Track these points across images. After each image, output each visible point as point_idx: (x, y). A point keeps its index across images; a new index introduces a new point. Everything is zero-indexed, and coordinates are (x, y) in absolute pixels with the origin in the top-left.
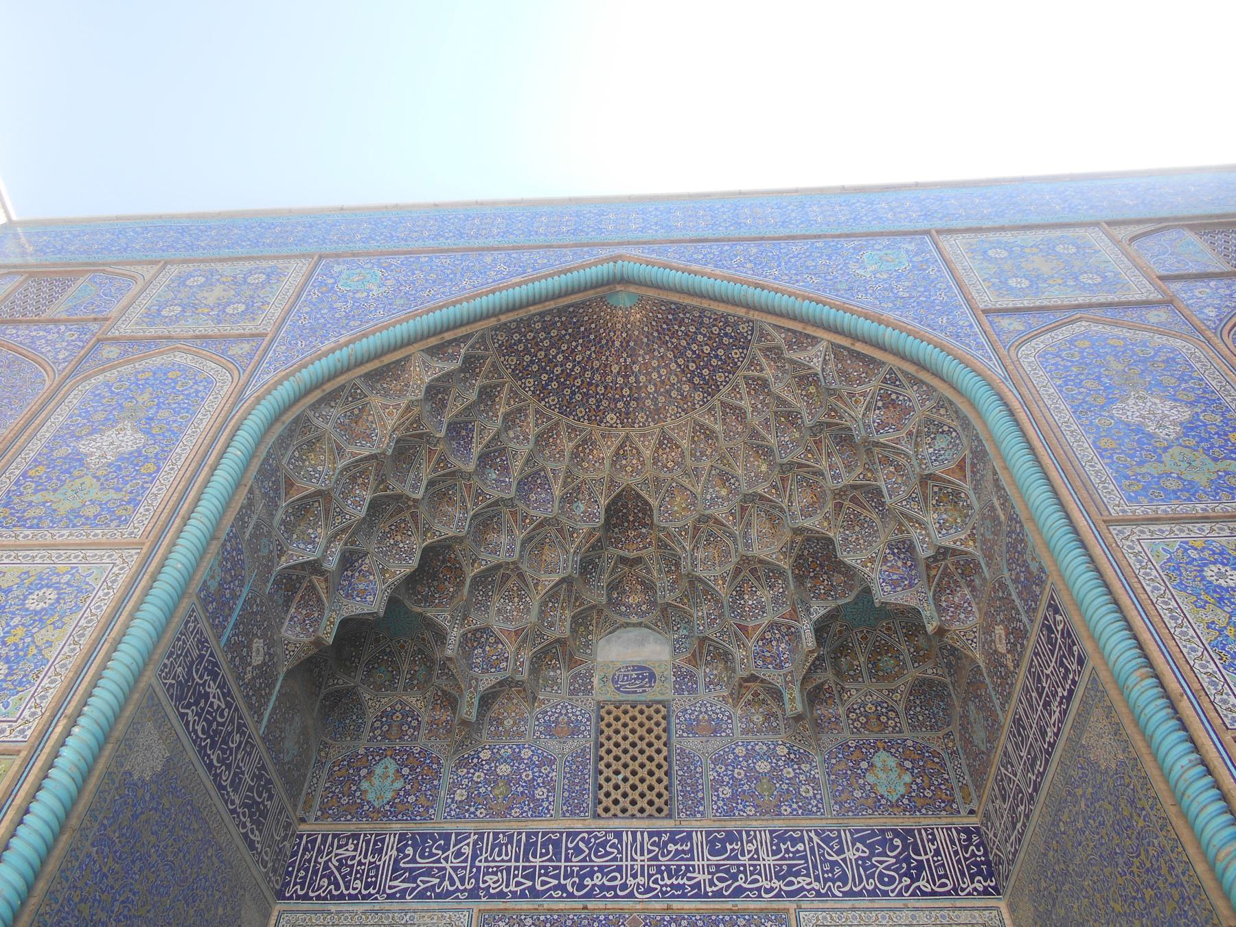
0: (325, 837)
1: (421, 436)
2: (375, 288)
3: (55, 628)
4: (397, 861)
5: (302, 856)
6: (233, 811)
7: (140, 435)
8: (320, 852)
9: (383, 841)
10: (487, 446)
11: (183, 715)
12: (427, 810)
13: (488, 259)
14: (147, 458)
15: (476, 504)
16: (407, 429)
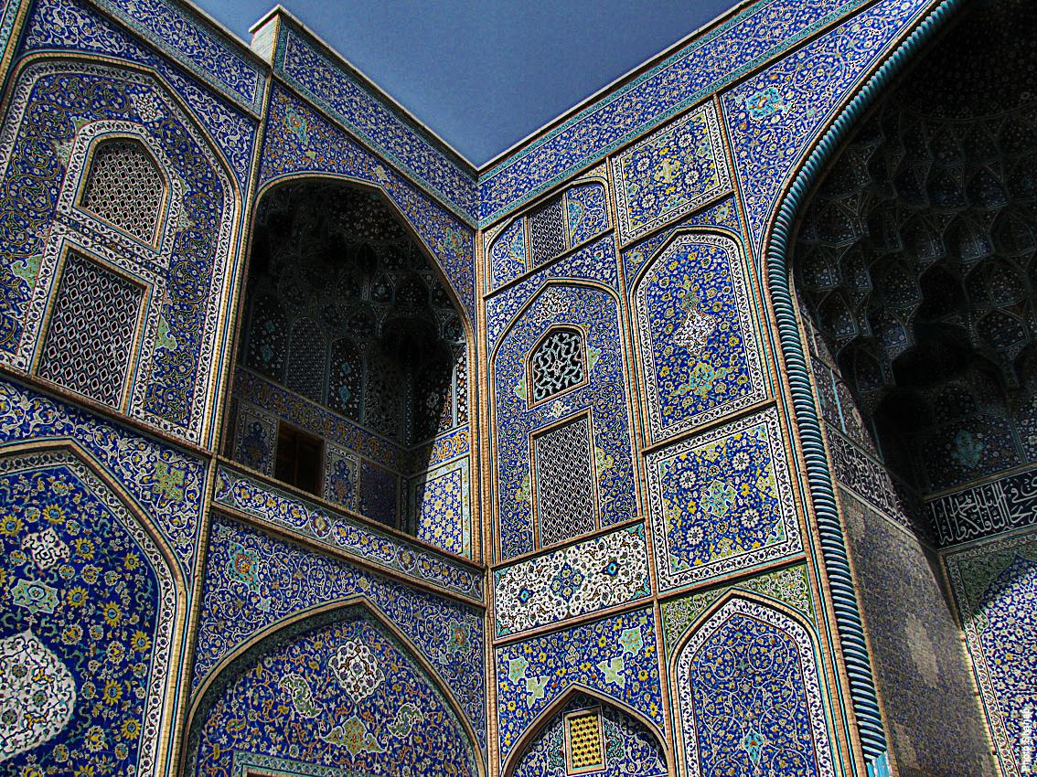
0: (946, 500)
1: (881, 206)
2: (782, 107)
3: (765, 477)
4: (1009, 500)
5: (938, 516)
6: (896, 519)
7: (708, 317)
8: (949, 511)
9: (990, 490)
10: (929, 178)
11: (855, 489)
12: (1012, 458)
13: (856, 28)
14: (726, 333)
15: (942, 227)
16: (870, 208)
